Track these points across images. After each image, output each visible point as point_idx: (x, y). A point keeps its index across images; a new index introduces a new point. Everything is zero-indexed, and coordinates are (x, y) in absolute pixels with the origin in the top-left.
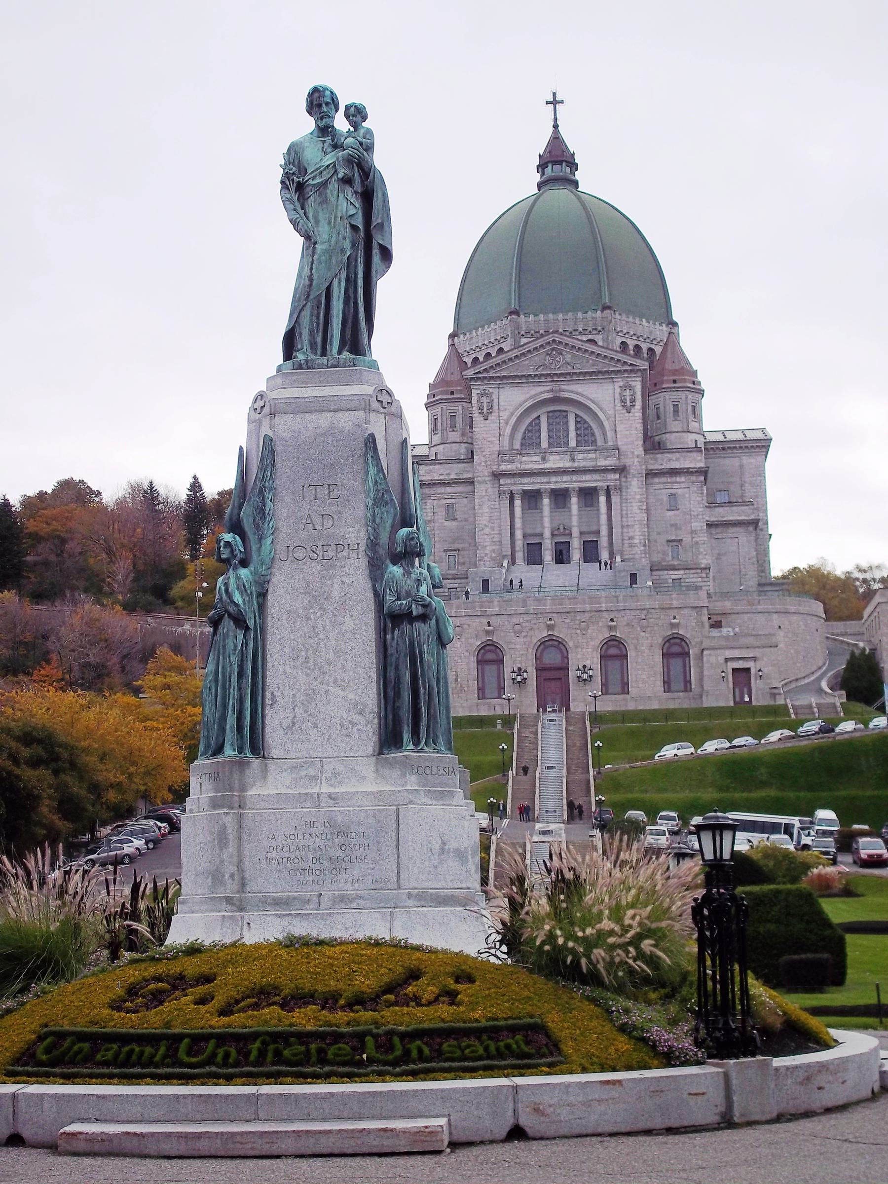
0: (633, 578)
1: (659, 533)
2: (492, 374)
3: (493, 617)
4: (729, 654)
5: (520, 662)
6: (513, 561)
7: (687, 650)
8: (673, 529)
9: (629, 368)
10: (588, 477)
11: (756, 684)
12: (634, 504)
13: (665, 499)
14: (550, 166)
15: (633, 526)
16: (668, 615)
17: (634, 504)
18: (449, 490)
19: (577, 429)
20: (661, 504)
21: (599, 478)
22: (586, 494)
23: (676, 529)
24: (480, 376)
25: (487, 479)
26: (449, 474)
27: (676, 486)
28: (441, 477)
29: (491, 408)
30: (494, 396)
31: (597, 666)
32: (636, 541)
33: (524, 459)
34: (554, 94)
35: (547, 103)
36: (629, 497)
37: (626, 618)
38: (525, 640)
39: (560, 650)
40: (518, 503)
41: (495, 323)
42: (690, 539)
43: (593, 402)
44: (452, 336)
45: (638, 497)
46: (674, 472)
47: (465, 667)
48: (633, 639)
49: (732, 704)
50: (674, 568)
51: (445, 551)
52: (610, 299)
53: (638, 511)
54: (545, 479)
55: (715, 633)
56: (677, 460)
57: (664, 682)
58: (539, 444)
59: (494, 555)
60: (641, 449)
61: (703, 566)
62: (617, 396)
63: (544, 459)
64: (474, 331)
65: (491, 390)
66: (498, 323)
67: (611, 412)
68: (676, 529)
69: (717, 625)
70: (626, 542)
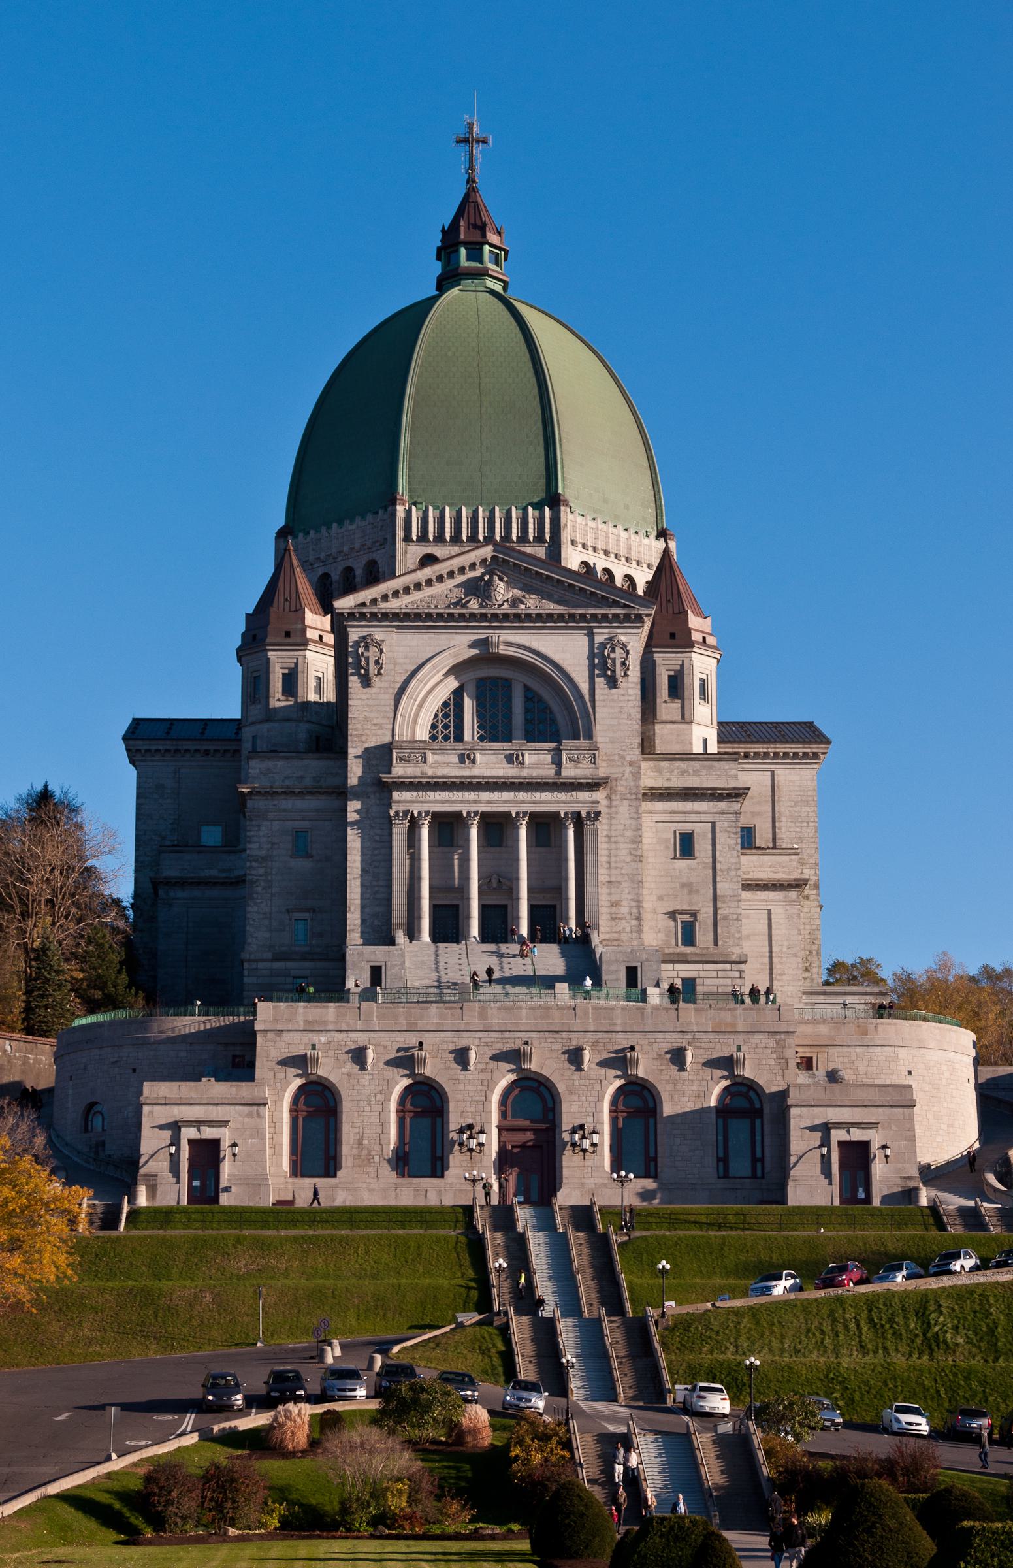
0: (632, 975)
1: (661, 898)
2: (383, 606)
3: (427, 1035)
4: (833, 1114)
5: (474, 1116)
6: (412, 933)
7: (757, 1105)
8: (686, 891)
9: (623, 612)
10: (545, 796)
11: (878, 1169)
12: (622, 846)
14: (463, 251)
15: (619, 882)
16: (728, 1044)
17: (622, 846)
18: (300, 804)
19: (527, 711)
20: (667, 847)
21: (564, 799)
22: (538, 824)
23: (690, 892)
24: (365, 610)
25: (370, 789)
26: (302, 777)
27: (693, 817)
28: (287, 782)
31: (606, 1128)
32: (624, 910)
33: (438, 758)
35: (459, 142)
36: (613, 833)
37: (656, 1046)
38: (482, 1076)
39: (541, 1095)
40: (425, 832)
41: (363, 517)
44: (282, 534)
45: (629, 834)
46: (689, 794)
47: (375, 1119)
48: (667, 1082)
49: (837, 1203)
50: (683, 959)
51: (288, 911)
52: (564, 488)
53: (628, 858)
54: (472, 796)
55: (802, 1078)
56: (696, 772)
57: (719, 1160)
58: (459, 737)
59: (376, 922)
60: (638, 751)
61: (734, 958)
64: (324, 529)
66: (370, 517)
67: (584, 687)
68: (690, 892)
69: (807, 1064)
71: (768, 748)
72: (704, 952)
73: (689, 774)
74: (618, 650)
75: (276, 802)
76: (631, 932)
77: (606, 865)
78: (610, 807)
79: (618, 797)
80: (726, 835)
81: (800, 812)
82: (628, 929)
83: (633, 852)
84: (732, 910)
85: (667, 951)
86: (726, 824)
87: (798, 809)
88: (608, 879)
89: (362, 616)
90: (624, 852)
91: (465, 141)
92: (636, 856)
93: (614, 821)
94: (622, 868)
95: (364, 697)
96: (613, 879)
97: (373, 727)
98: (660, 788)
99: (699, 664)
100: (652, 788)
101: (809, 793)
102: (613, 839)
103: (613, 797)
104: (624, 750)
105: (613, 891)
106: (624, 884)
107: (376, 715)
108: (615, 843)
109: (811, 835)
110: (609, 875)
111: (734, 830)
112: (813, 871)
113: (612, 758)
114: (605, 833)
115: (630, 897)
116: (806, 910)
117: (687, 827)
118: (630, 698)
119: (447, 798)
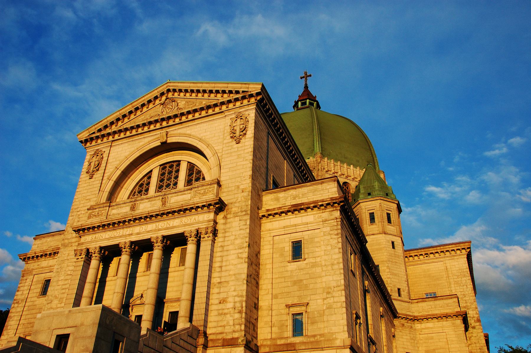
8: (296, 288)
12: (232, 252)
13: (288, 249)
14: (300, 103)
15: (227, 282)
20: (282, 255)
30: (105, 156)
34: (306, 73)
36: (226, 243)
42: (320, 302)
43: (200, 140)
45: (238, 242)
46: (297, 209)
54: (126, 231)
62: (228, 129)
63: (133, 208)
65: (103, 150)
71: (437, 250)
72: (312, 339)
73: (299, 198)
74: (239, 120)
75: (39, 263)
77: (218, 269)
78: (225, 224)
79: (232, 216)
80: (329, 237)
81: (461, 281)
82: (231, 323)
83: (240, 255)
84: (336, 299)
85: (279, 342)
86: (328, 229)
87: (460, 279)
88: (219, 280)
89: (92, 139)
90: (234, 257)
91: (303, 77)
92: (242, 258)
93: (227, 234)
94: (230, 271)
95: (86, 185)
96: (223, 280)
97: (86, 201)
98: (274, 209)
99: (385, 206)
100: (268, 210)
101: (465, 270)
102: (225, 248)
103: (228, 216)
104: (240, 182)
105: (222, 290)
106: (231, 283)
107: (89, 194)
109: (470, 292)
110: (220, 277)
111: (336, 232)
112: (475, 312)
113: (230, 189)
114: (220, 244)
115: (235, 294)
116: (474, 335)
117: (296, 237)
118: (246, 147)
119: (113, 236)
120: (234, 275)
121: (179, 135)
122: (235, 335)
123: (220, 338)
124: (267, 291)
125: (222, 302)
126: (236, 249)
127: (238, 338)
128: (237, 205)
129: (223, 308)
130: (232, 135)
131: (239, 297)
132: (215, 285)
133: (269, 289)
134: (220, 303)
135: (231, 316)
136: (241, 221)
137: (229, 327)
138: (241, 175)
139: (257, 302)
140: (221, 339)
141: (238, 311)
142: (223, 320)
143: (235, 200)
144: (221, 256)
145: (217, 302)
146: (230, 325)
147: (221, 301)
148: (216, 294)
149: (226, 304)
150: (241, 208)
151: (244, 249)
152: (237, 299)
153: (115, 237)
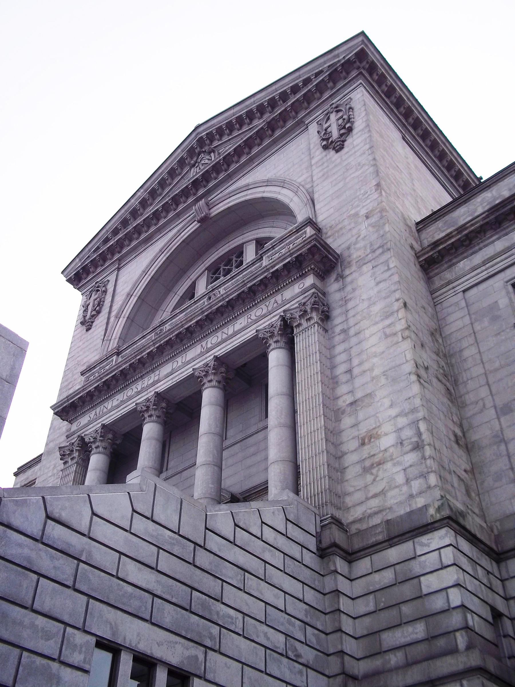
17: (367, 333)
29: (100, 304)
70: (351, 459)
76: (408, 481)
79: (354, 268)
82: (400, 479)
83: (388, 331)
88: (349, 399)
92: (395, 334)
93: (350, 305)
94: (371, 370)
96: (359, 394)
102: (352, 332)
105: (361, 415)
106: (380, 394)
108: (357, 334)
110: (351, 392)
115: (393, 412)
120: (384, 373)
121: (228, 196)
122: (416, 503)
123: (379, 521)
124: (481, 403)
125: (366, 441)
126: (376, 323)
127: (426, 507)
128: (361, 244)
129: (372, 453)
130: (325, 143)
131: (406, 415)
132: (344, 410)
133: (482, 399)
134: (363, 444)
135: (394, 465)
136: (376, 269)
137: (397, 490)
138: (358, 194)
139: (459, 433)
140: (382, 523)
141: (410, 447)
142: (378, 479)
143: (354, 238)
144: (345, 351)
145: (353, 445)
146: (397, 484)
147: (363, 440)
148: (349, 429)
149: (377, 442)
150: (371, 245)
151: (396, 315)
152: (402, 421)
153: (130, 398)
